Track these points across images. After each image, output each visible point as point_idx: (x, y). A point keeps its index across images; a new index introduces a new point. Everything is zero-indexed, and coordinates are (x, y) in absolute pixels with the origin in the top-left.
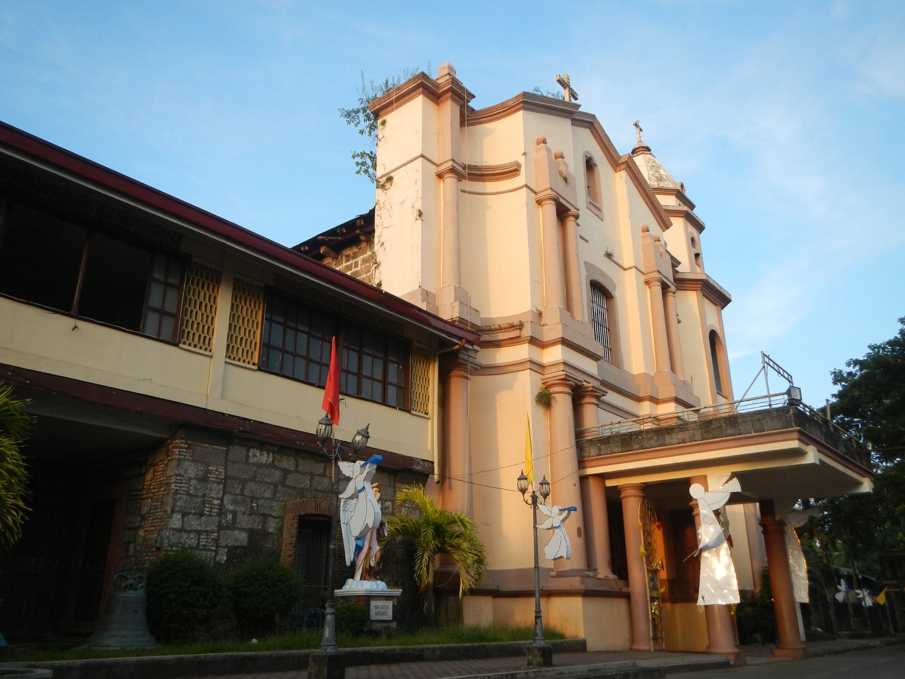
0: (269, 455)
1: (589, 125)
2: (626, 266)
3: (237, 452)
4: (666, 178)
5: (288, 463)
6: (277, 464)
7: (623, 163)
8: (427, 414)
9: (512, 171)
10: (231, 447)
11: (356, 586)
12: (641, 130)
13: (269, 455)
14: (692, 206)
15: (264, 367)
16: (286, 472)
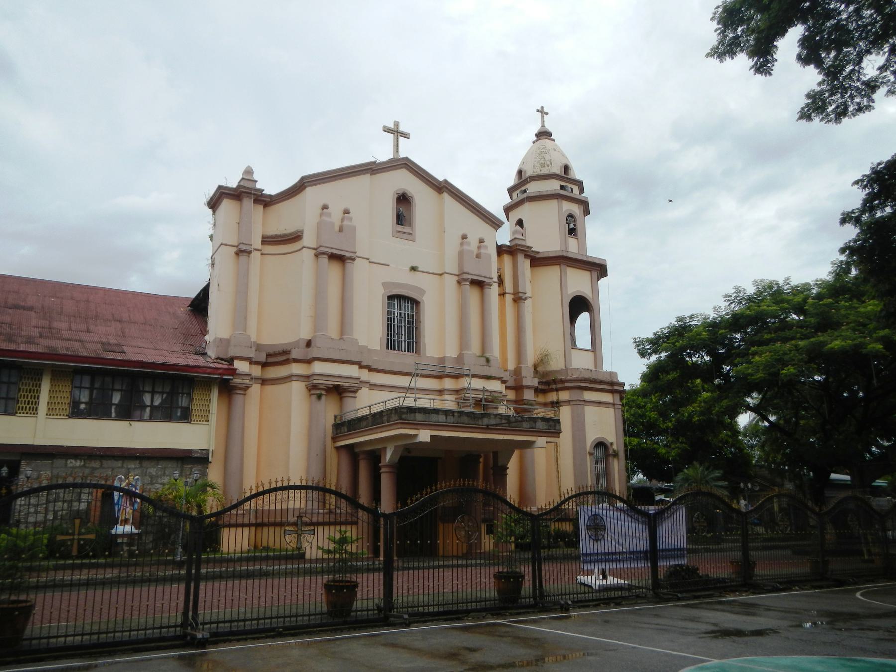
0: (81, 461)
1: (404, 165)
2: (440, 273)
3: (59, 462)
4: (549, 163)
5: (95, 464)
6: (87, 465)
7: (442, 187)
8: (208, 421)
9: (296, 237)
10: (55, 461)
11: (120, 529)
12: (547, 114)
13: (81, 461)
14: (580, 184)
15: (70, 416)
16: (94, 469)
